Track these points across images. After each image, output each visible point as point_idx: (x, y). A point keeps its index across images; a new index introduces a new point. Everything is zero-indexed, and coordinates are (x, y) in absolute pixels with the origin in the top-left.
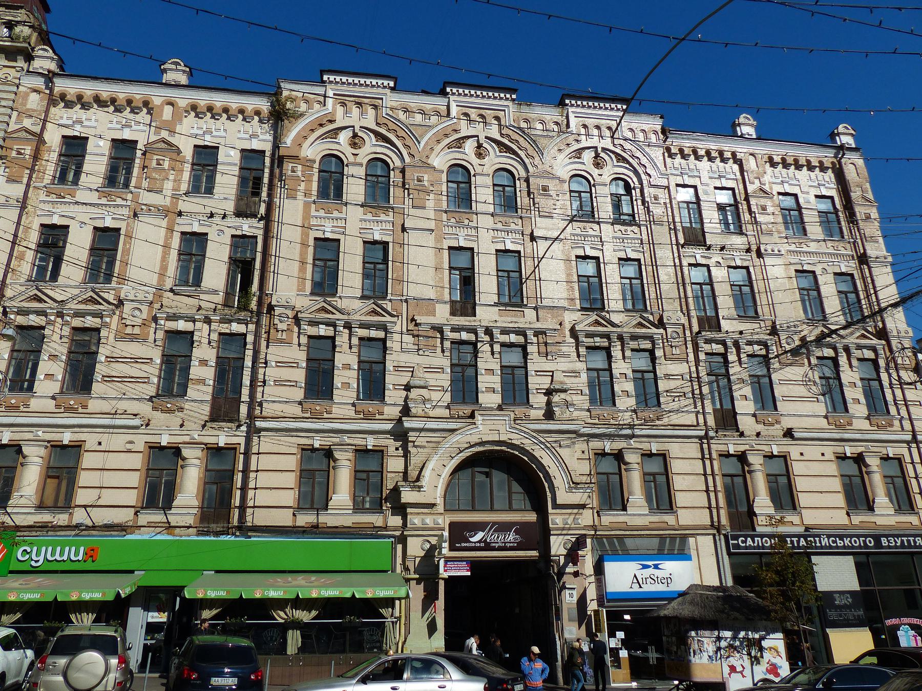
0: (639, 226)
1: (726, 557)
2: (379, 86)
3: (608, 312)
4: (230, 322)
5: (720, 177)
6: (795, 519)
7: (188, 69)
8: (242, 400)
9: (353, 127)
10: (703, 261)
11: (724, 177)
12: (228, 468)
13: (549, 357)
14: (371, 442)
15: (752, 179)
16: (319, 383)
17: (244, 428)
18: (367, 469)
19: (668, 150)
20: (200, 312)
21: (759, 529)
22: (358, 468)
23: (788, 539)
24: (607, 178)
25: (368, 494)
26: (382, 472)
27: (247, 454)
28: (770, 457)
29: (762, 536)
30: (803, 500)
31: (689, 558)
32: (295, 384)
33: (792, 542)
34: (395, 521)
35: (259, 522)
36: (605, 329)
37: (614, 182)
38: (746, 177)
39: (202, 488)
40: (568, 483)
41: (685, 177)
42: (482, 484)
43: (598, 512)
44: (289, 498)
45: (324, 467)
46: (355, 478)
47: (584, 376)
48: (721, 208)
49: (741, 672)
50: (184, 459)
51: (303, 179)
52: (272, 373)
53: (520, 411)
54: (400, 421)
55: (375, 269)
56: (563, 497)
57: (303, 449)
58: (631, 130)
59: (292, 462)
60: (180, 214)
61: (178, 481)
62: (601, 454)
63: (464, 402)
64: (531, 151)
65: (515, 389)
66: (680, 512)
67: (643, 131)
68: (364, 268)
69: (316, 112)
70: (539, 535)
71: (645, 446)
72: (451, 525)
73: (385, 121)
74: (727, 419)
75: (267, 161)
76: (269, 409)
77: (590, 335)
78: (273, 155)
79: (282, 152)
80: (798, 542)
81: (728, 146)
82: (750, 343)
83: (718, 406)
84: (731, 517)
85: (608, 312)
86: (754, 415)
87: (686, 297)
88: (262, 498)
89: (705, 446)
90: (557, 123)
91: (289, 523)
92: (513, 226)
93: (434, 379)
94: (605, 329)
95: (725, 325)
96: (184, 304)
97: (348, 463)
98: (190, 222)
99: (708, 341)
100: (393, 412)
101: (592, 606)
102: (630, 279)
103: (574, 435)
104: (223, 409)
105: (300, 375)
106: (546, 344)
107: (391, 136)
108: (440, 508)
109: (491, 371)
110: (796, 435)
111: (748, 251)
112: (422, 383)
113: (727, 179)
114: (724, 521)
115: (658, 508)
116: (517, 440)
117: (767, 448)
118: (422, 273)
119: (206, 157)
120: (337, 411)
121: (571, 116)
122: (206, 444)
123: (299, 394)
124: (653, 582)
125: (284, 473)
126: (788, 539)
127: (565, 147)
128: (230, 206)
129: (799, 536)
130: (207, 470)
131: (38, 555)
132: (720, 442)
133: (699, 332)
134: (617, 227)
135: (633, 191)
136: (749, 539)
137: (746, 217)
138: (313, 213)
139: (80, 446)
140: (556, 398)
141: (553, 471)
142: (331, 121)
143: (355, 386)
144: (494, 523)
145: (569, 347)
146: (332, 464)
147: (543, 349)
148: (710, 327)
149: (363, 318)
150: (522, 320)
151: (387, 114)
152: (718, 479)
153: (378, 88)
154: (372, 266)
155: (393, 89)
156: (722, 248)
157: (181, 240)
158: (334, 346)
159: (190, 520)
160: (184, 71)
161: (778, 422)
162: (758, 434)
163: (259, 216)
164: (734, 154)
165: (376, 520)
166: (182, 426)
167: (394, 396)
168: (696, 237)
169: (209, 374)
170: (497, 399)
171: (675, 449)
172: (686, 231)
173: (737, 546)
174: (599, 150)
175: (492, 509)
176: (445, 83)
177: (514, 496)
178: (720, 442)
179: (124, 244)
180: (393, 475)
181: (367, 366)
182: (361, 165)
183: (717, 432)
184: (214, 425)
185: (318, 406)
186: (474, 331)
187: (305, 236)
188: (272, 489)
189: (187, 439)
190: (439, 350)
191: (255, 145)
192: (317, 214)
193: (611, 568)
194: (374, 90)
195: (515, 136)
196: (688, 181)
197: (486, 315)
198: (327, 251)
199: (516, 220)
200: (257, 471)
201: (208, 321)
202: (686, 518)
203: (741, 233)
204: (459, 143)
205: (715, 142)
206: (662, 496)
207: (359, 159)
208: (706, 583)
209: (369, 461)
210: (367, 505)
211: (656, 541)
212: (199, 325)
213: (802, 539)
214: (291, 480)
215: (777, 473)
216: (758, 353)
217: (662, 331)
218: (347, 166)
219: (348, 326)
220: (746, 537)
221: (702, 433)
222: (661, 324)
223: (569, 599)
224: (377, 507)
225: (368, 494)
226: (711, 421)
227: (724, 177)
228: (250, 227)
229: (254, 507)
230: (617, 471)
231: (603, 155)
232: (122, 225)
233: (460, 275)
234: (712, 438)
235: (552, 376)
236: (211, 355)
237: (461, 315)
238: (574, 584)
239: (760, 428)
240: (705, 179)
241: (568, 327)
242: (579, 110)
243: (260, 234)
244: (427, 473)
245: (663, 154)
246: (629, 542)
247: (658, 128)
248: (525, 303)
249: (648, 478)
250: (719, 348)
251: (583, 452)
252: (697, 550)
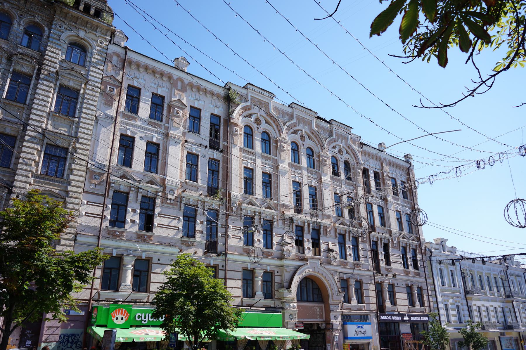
24: (343, 160)
59: (240, 275)
74: (377, 268)
104: (211, 247)
131: (145, 318)
139: (149, 260)
163: (220, 150)
179: (163, 153)
191: (216, 112)
209: (268, 277)
232: (161, 143)
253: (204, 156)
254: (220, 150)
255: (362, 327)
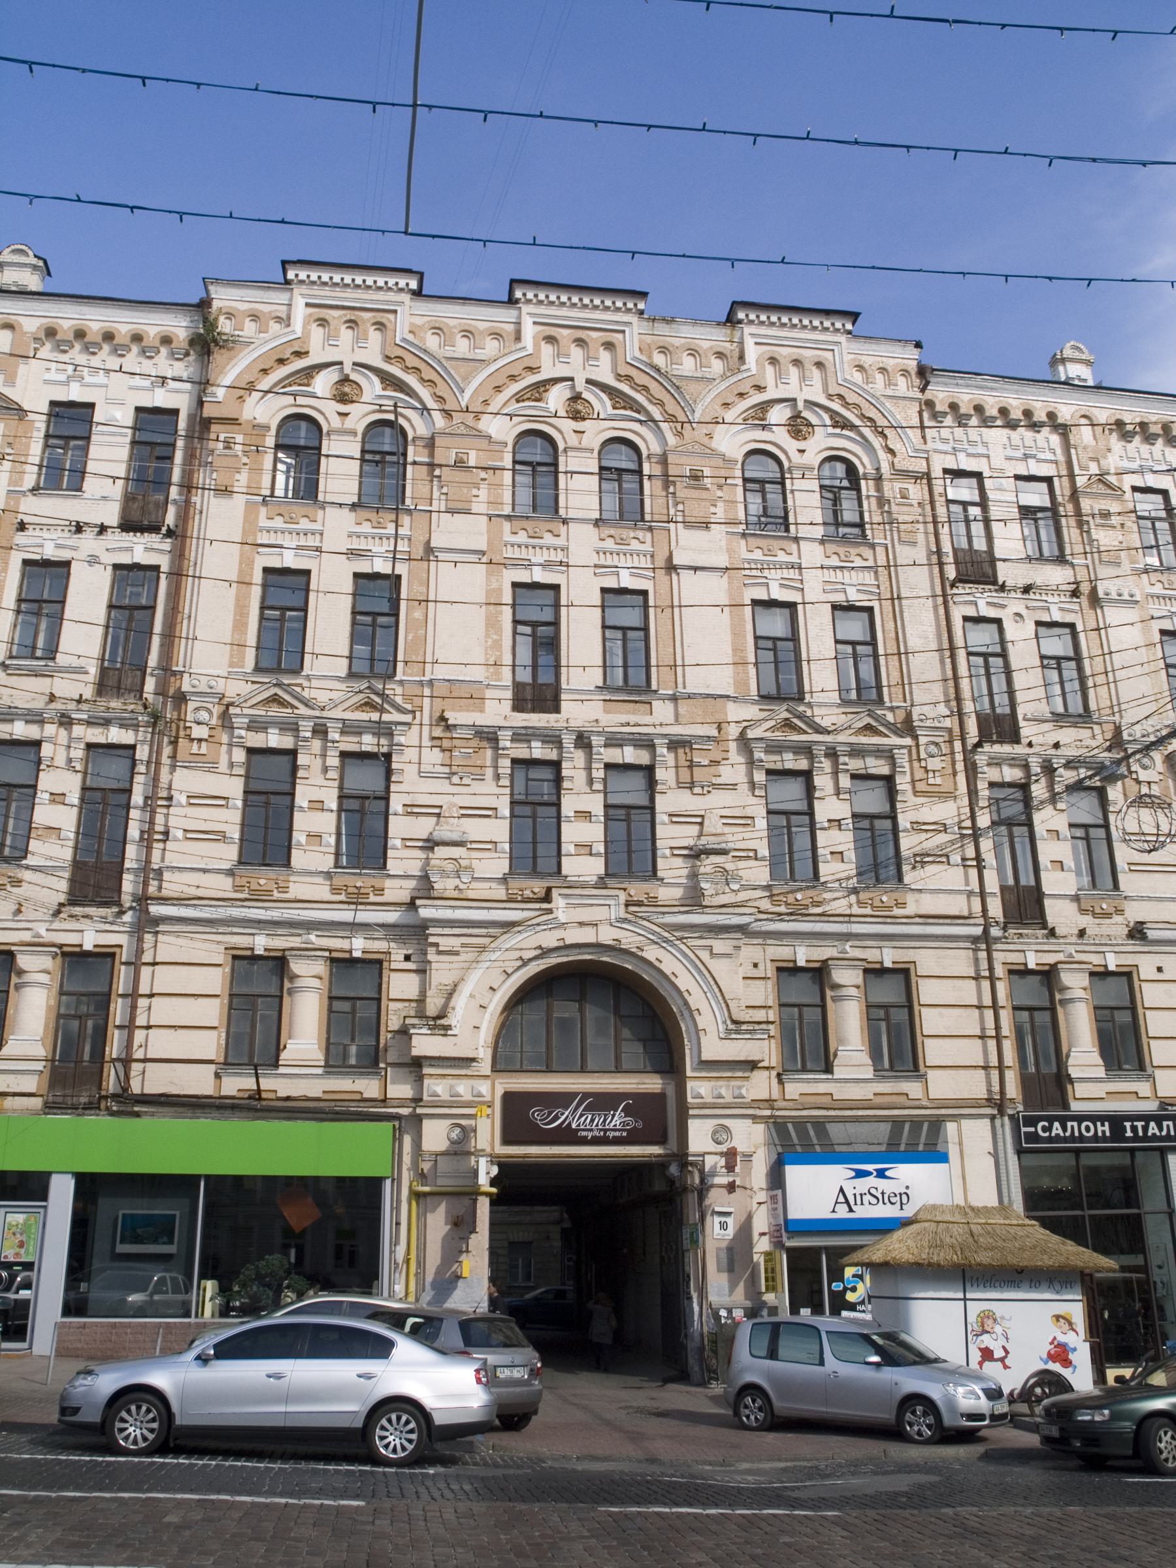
0: (873, 546)
1: (1013, 1160)
2: (390, 289)
3: (810, 705)
4: (106, 723)
5: (1026, 457)
6: (1144, 1088)
7: (41, 263)
8: (127, 865)
9: (341, 363)
10: (992, 613)
11: (1034, 456)
12: (99, 989)
13: (697, 790)
14: (359, 946)
15: (1084, 461)
16: (266, 836)
17: (128, 917)
18: (352, 995)
19: (930, 404)
20: (53, 706)
21: (1076, 1107)
22: (334, 994)
23: (1128, 1124)
24: (813, 457)
25: (353, 1040)
26: (379, 1000)
27: (135, 964)
28: (1100, 975)
29: (1080, 1119)
30: (1159, 1052)
31: (943, 1158)
32: (222, 837)
33: (1134, 1129)
34: (400, 1090)
35: (151, 1089)
36: (803, 738)
37: (827, 465)
38: (1074, 457)
39: (52, 1025)
40: (724, 1022)
41: (961, 456)
42: (565, 1024)
43: (779, 1075)
44: (210, 1045)
45: (274, 991)
46: (330, 1011)
47: (761, 823)
48: (1027, 513)
49: (1002, 1360)
50: (21, 973)
51: (245, 460)
52: (179, 818)
53: (637, 890)
54: (412, 905)
55: (374, 625)
56: (714, 1047)
57: (235, 957)
58: (860, 368)
59: (215, 980)
60: (22, 527)
61: (10, 1011)
62: (787, 971)
63: (535, 873)
64: (671, 407)
65: (631, 846)
66: (931, 1074)
67: (883, 370)
68: (354, 623)
69: (275, 337)
70: (658, 1118)
71: (872, 955)
72: (510, 1099)
73: (400, 352)
74: (1026, 906)
75: (182, 424)
76: (173, 884)
77: (774, 748)
78: (191, 418)
79: (208, 411)
80: (1145, 1129)
81: (1041, 402)
82: (1069, 764)
83: (1011, 882)
84: (1026, 1081)
85: (810, 705)
86: (1076, 898)
87: (956, 678)
88: (160, 1044)
89: (983, 955)
90: (720, 355)
91: (209, 1091)
92: (635, 545)
93: (476, 829)
94: (803, 738)
95: (1027, 731)
96: (26, 691)
97: (316, 983)
98: (39, 541)
99: (996, 762)
100: (398, 890)
101: (762, 1245)
102: (853, 643)
103: (739, 935)
105: (230, 820)
106: (691, 765)
107: (411, 380)
108: (485, 1067)
109: (586, 815)
110: (1151, 934)
111: (1075, 593)
112: (455, 837)
113: (1039, 461)
114: (1013, 1090)
115: (892, 1069)
116: (629, 939)
117: (1096, 959)
118: (460, 636)
119: (71, 421)
120: (298, 888)
121: (749, 343)
122: (61, 946)
123: (230, 853)
124: (874, 1201)
125: (200, 1000)
126: (1128, 1124)
127: (736, 399)
128: (111, 514)
129: (1146, 1118)
130: (62, 993)
132: (1011, 947)
133: (979, 745)
134: (831, 548)
135: (863, 482)
136: (1056, 1124)
137: (1071, 533)
138: (263, 522)
140: (708, 865)
141: (696, 999)
142: (299, 354)
143: (332, 840)
144: (586, 1095)
145: (734, 770)
146: (287, 984)
147: (685, 775)
148: (999, 734)
149: (348, 715)
150: (647, 719)
151: (404, 340)
152: (1005, 1017)
153: (390, 292)
154: (369, 619)
155: (418, 294)
156: (1027, 589)
157: (23, 576)
158: (295, 768)
159: (30, 1084)
160: (35, 267)
161: (1120, 911)
162: (1082, 933)
163: (164, 530)
164: (1051, 416)
165: (369, 1087)
166: (19, 911)
167: (403, 861)
168: (978, 570)
169: (66, 819)
170: (594, 867)
171: (926, 960)
172: (960, 555)
173: (1033, 1137)
174: (800, 405)
175: (583, 1070)
176: (513, 281)
177: (625, 1047)
178: (1011, 947)
180: (399, 1005)
181: (354, 804)
182: (355, 434)
183: (1005, 929)
184: (78, 910)
185: (264, 878)
186: (553, 738)
187: (246, 563)
188: (178, 1028)
189: (26, 936)
190: (489, 772)
191: (161, 399)
192: (270, 524)
193: (795, 1174)
194: (381, 296)
195: (641, 379)
196: (967, 464)
197: (580, 710)
198: (285, 595)
199: (640, 534)
200: (151, 996)
201: (66, 721)
202: (942, 1086)
203: (1061, 559)
204: (539, 389)
205: (1017, 392)
206: (898, 1046)
207: (349, 423)
208: (977, 1202)
210: (353, 1061)
211: (885, 1129)
212: (50, 729)
213: (1152, 1124)
214: (212, 1012)
215: (1113, 1004)
216: (1088, 783)
217: (908, 741)
218: (328, 434)
219: (320, 731)
220: (1051, 1120)
221: (978, 931)
222: (908, 727)
223: (718, 1234)
224: (371, 1062)
225: (353, 1040)
226: (996, 909)
227: (1034, 456)
228: (144, 549)
229: (145, 1060)
230: (818, 1001)
231: (806, 414)
233: (534, 635)
234: (997, 940)
235: (701, 824)
236: (71, 785)
237: (533, 710)
238: (729, 1205)
239: (1086, 921)
240: (998, 461)
241: (733, 731)
242: (763, 330)
243: (164, 562)
244: (460, 1002)
245: (920, 413)
246: (832, 1129)
247: (912, 365)
248: (654, 687)
249: (875, 1014)
250: (1011, 774)
251: (755, 965)
252: (960, 1144)
253: (93, 560)
254: (164, 530)
255: (881, 1174)
